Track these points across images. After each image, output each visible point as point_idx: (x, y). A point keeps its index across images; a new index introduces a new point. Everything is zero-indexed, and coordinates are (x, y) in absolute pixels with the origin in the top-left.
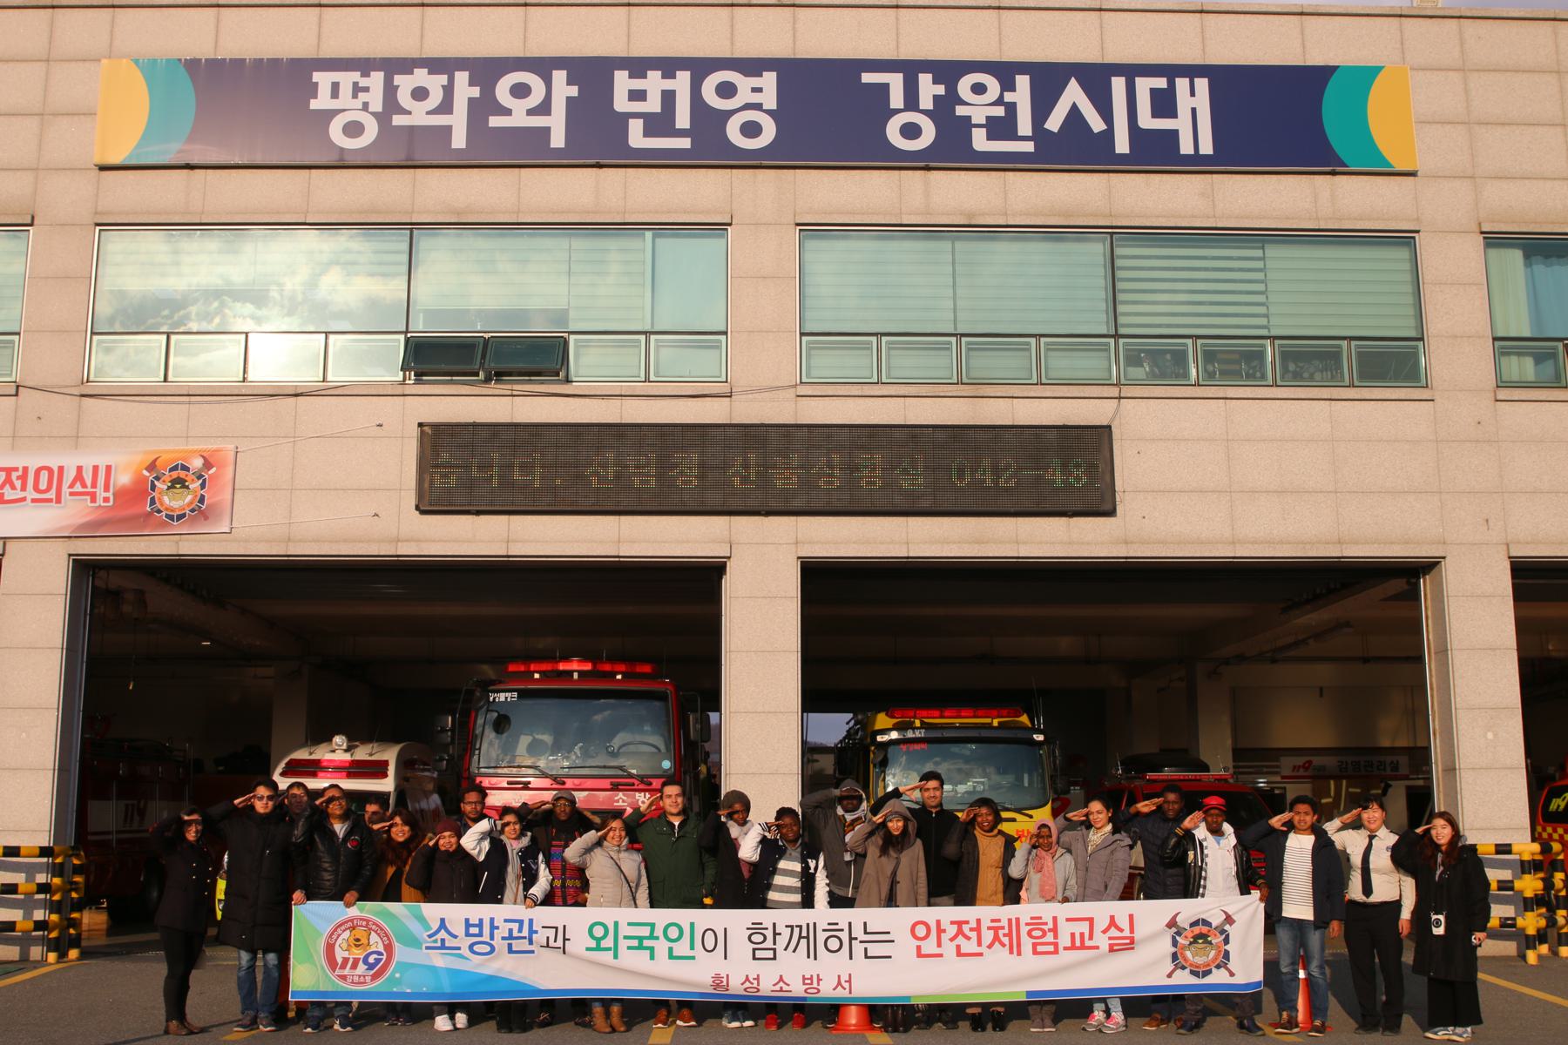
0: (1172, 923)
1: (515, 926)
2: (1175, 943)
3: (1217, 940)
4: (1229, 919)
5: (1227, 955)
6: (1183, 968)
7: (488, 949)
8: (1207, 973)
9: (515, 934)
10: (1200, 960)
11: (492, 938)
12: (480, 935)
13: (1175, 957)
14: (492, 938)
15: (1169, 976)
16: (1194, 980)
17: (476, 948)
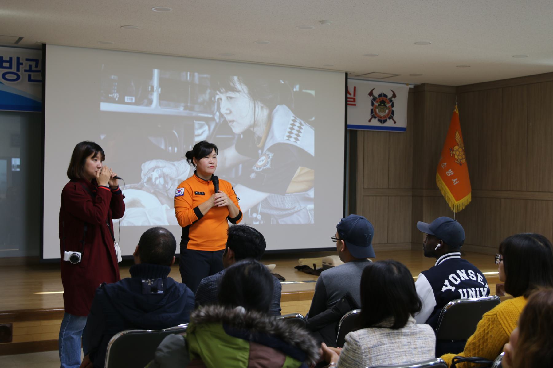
0: (371, 94)
1: (33, 64)
2: (373, 104)
3: (389, 105)
4: (394, 96)
5: (393, 113)
6: (375, 118)
7: (15, 77)
8: (385, 121)
9: (33, 68)
10: (382, 114)
11: (18, 70)
12: (10, 67)
13: (372, 111)
14: (18, 70)
15: (370, 121)
16: (379, 124)
17: (7, 76)
